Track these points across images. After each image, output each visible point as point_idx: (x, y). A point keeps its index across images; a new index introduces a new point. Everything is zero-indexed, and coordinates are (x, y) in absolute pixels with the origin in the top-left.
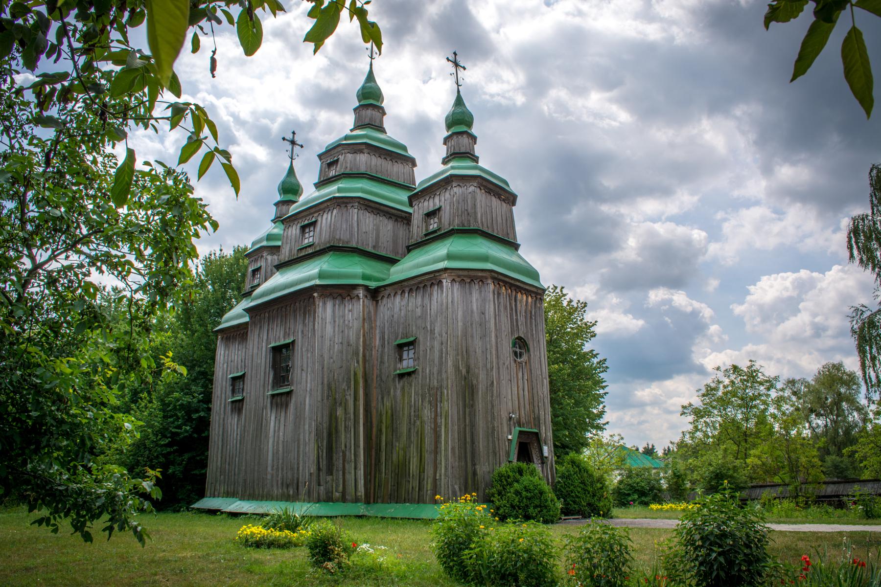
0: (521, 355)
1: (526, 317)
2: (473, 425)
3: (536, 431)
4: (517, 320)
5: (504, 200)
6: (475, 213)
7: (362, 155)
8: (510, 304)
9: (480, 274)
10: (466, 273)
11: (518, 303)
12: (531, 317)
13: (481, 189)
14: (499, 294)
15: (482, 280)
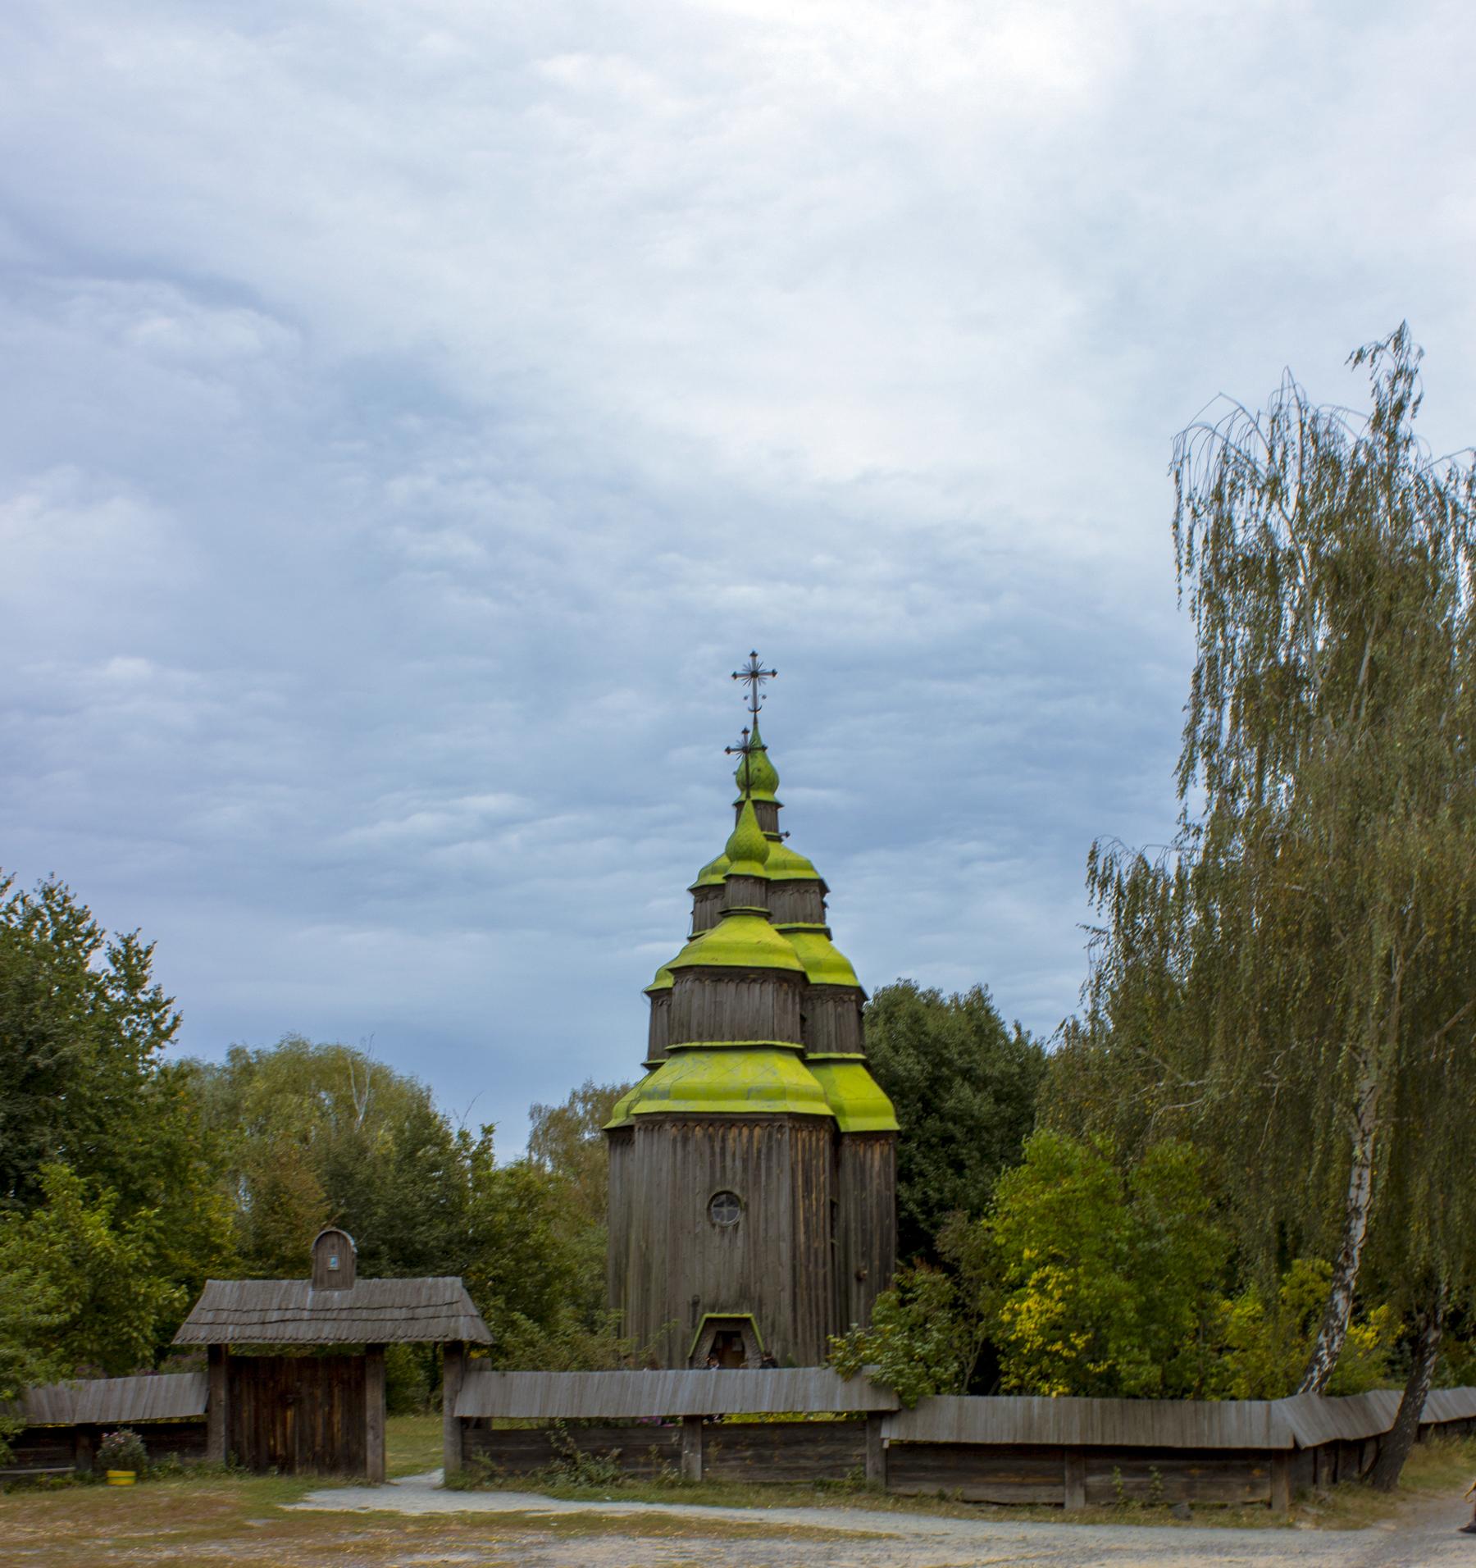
0: (731, 1216)
1: (745, 1161)
2: (647, 1314)
3: (747, 1315)
4: (724, 1168)
5: (754, 981)
6: (689, 1022)
7: (708, 902)
8: (712, 1148)
9: (660, 1118)
10: (648, 1118)
11: (730, 1143)
12: (759, 1157)
13: (700, 981)
14: (685, 1140)
15: (661, 1124)
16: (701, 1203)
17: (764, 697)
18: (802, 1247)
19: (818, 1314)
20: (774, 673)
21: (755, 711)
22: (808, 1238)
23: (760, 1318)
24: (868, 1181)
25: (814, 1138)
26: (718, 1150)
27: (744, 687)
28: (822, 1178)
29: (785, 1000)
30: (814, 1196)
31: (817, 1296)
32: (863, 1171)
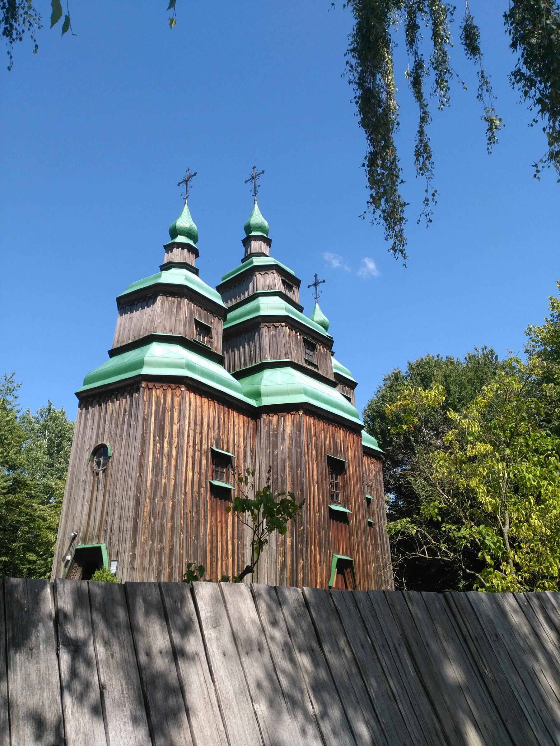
5: (150, 298)
12: (124, 414)
16: (87, 456)
17: (259, 186)
18: (149, 483)
19: (161, 541)
20: (263, 172)
21: (255, 195)
22: (157, 474)
23: (109, 549)
24: (279, 442)
25: (169, 396)
26: (103, 414)
27: (250, 185)
28: (176, 427)
29: (170, 308)
30: (166, 440)
31: (162, 526)
32: (276, 436)
